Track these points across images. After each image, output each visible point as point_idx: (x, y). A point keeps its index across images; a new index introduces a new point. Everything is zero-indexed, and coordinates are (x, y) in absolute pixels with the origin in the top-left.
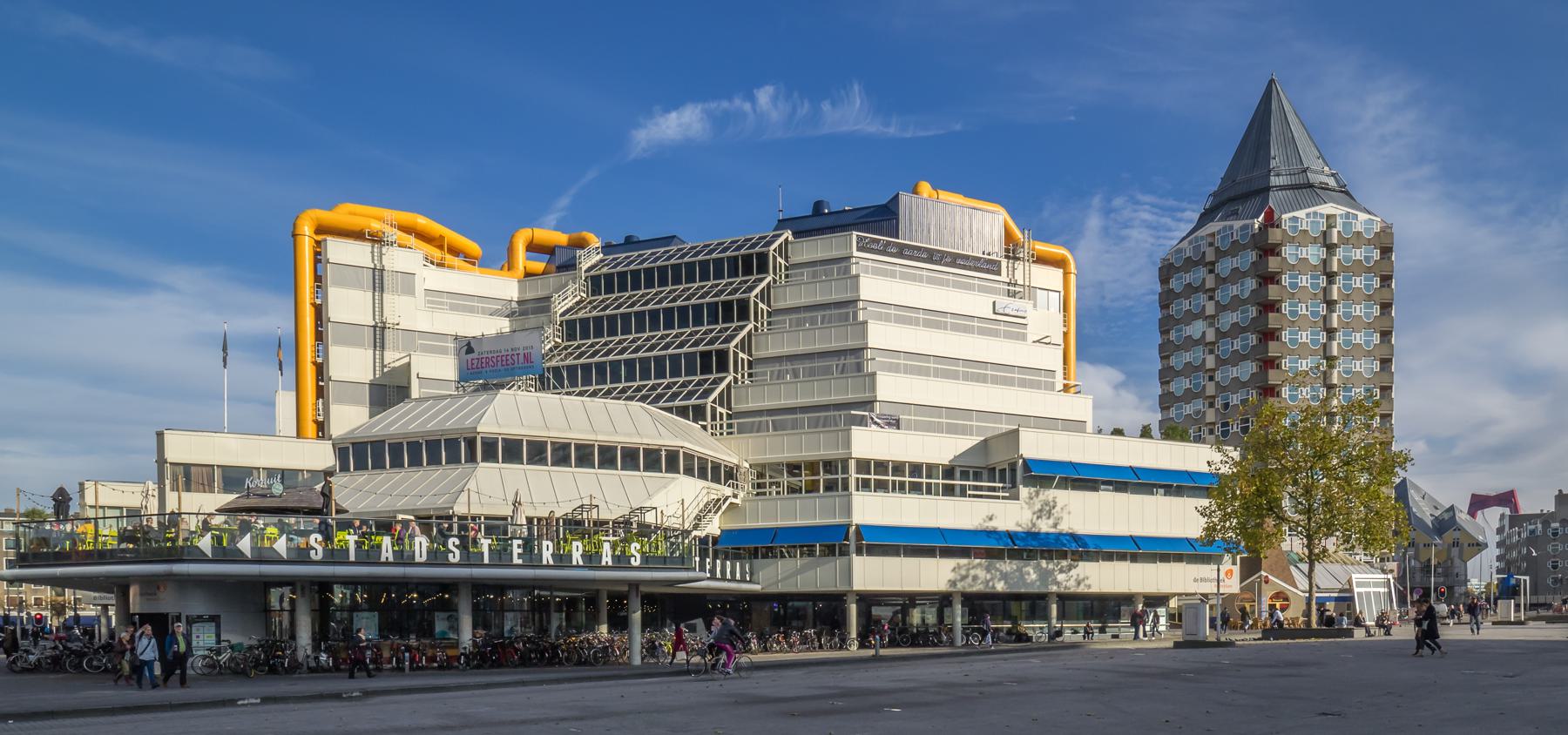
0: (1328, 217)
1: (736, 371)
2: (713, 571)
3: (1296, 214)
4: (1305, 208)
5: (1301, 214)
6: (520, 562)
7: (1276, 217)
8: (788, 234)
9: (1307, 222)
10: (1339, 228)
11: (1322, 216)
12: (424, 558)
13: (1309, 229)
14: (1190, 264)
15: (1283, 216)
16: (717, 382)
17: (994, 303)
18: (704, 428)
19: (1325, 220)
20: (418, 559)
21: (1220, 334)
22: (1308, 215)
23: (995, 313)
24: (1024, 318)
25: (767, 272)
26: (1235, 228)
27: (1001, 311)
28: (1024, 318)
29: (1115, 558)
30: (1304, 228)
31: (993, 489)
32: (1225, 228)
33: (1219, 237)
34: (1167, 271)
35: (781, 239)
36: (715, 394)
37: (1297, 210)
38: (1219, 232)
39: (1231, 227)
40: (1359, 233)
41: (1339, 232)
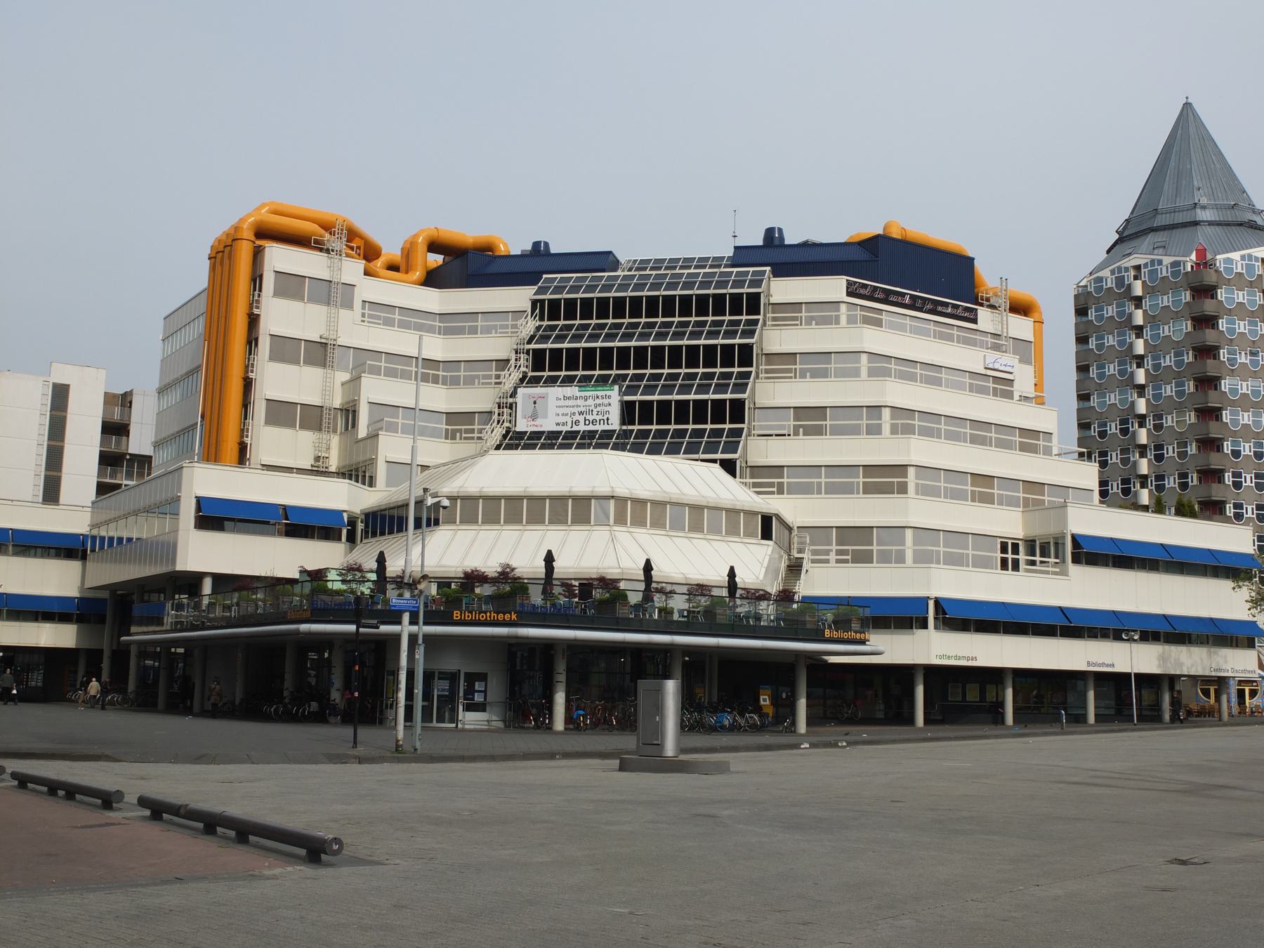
3: (1231, 255)
4: (1239, 250)
5: (1236, 256)
7: (1209, 256)
9: (1242, 264)
11: (1257, 259)
13: (1244, 272)
15: (1218, 257)
17: (985, 356)
19: (1260, 264)
22: (1243, 258)
24: (1011, 373)
26: (1164, 263)
27: (991, 366)
28: (1011, 373)
29: (1162, 639)
30: (1239, 270)
32: (1153, 261)
33: (1146, 270)
37: (1231, 252)
38: (1146, 265)
39: (1160, 262)
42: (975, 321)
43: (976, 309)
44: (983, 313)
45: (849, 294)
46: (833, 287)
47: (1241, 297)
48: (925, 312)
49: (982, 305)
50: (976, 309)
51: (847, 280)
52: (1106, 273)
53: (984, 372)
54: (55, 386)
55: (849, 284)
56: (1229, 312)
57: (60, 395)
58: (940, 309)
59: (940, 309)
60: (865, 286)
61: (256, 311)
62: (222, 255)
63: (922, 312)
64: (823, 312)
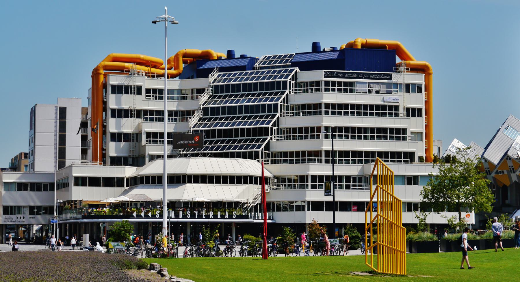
1: (271, 135)
2: (255, 217)
6: (205, 217)
8: (297, 69)
12: (181, 217)
16: (273, 116)
18: (258, 161)
20: (180, 217)
23: (384, 102)
25: (286, 89)
28: (398, 102)
31: (361, 186)
42: (391, 79)
43: (392, 74)
44: (394, 75)
45: (325, 77)
46: (319, 75)
48: (364, 79)
49: (393, 72)
50: (392, 74)
51: (325, 71)
53: (383, 103)
54: (60, 108)
55: (325, 72)
57: (63, 112)
58: (371, 77)
59: (371, 77)
61: (105, 100)
62: (95, 74)
63: (363, 79)
64: (315, 86)
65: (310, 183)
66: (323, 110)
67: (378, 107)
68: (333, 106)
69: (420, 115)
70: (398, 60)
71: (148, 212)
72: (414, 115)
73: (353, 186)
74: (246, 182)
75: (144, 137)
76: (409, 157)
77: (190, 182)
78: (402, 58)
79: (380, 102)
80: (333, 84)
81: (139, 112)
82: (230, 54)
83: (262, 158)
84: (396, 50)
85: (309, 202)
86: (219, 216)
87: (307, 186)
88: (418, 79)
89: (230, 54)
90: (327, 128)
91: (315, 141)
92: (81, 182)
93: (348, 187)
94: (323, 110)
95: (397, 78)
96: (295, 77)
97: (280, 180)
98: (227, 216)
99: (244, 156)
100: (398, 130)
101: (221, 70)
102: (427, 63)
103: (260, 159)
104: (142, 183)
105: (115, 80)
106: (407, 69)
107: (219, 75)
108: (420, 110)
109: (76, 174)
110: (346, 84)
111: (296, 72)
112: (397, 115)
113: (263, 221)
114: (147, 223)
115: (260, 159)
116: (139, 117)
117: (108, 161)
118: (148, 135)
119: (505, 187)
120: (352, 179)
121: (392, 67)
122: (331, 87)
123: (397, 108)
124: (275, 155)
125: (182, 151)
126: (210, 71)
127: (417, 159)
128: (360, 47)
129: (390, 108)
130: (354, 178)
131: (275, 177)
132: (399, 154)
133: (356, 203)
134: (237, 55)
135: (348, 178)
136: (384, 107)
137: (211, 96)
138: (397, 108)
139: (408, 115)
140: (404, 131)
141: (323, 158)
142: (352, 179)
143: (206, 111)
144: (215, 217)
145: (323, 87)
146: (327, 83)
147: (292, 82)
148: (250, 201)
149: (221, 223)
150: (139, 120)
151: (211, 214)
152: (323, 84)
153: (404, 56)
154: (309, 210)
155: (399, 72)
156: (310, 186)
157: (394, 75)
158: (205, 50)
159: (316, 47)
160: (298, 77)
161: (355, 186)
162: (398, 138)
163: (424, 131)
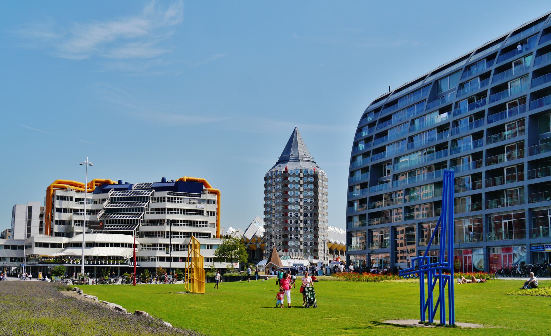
0: (301, 170)
1: (140, 223)
2: (130, 264)
8: (154, 190)
10: (303, 172)
11: (299, 170)
14: (270, 178)
16: (141, 214)
18: (133, 236)
19: (300, 171)
21: (276, 198)
25: (148, 200)
30: (294, 173)
31: (184, 249)
34: (265, 179)
35: (152, 192)
36: (150, 194)
40: (308, 174)
41: (303, 174)
42: (200, 197)
44: (202, 195)
46: (165, 194)
47: (294, 179)
52: (269, 173)
53: (196, 209)
54: (29, 207)
55: (168, 193)
56: (291, 183)
57: (30, 209)
60: (172, 193)
62: (49, 190)
64: (163, 199)
65: (159, 248)
66: (166, 211)
67: (194, 210)
68: (172, 209)
69: (214, 215)
70: (204, 188)
71: (74, 261)
72: (211, 215)
73: (180, 249)
74: (126, 247)
75: (73, 223)
76: (208, 235)
77: (97, 246)
78: (206, 187)
79: (195, 208)
80: (172, 198)
81: (71, 210)
82: (120, 182)
83: (135, 234)
84: (203, 183)
85: (158, 257)
86: (111, 264)
87: (157, 249)
88: (214, 197)
89: (120, 182)
90: (168, 220)
91: (162, 226)
92: (39, 245)
93: (178, 250)
94: (166, 211)
95: (203, 197)
96: (153, 195)
97: (144, 246)
98: (115, 264)
99: (125, 233)
100: (203, 222)
101: (115, 189)
102: (218, 190)
103: (134, 235)
104: (71, 246)
105: (59, 193)
106: (208, 192)
107: (114, 192)
108: (214, 212)
109: (36, 241)
110: (178, 199)
111: (153, 192)
112: (203, 215)
113: (134, 266)
114: (73, 267)
115: (134, 235)
116: (71, 212)
117: (54, 234)
118: (76, 222)
119: (254, 251)
120: (180, 246)
121: (201, 191)
122: (171, 200)
123: (203, 211)
124: (141, 233)
125: (93, 230)
126: (109, 190)
127: (212, 236)
128: (185, 181)
129: (200, 211)
130: (181, 246)
131: (141, 244)
132: (203, 234)
133: (181, 258)
134: (124, 183)
135: (178, 245)
136: (197, 211)
137: (109, 203)
138: (203, 211)
139: (208, 215)
140: (206, 222)
141: (166, 235)
142: (180, 246)
143: (106, 210)
144: (109, 264)
145: (167, 200)
146: (169, 198)
147: (151, 197)
148: (128, 256)
149: (112, 267)
150: (71, 214)
151: (107, 262)
152: (167, 198)
153: (207, 186)
154: (158, 261)
155: (204, 194)
156: (158, 249)
157: (202, 195)
158: (107, 179)
159: (163, 180)
160: (154, 194)
161: (181, 249)
162: (203, 226)
163: (216, 223)
